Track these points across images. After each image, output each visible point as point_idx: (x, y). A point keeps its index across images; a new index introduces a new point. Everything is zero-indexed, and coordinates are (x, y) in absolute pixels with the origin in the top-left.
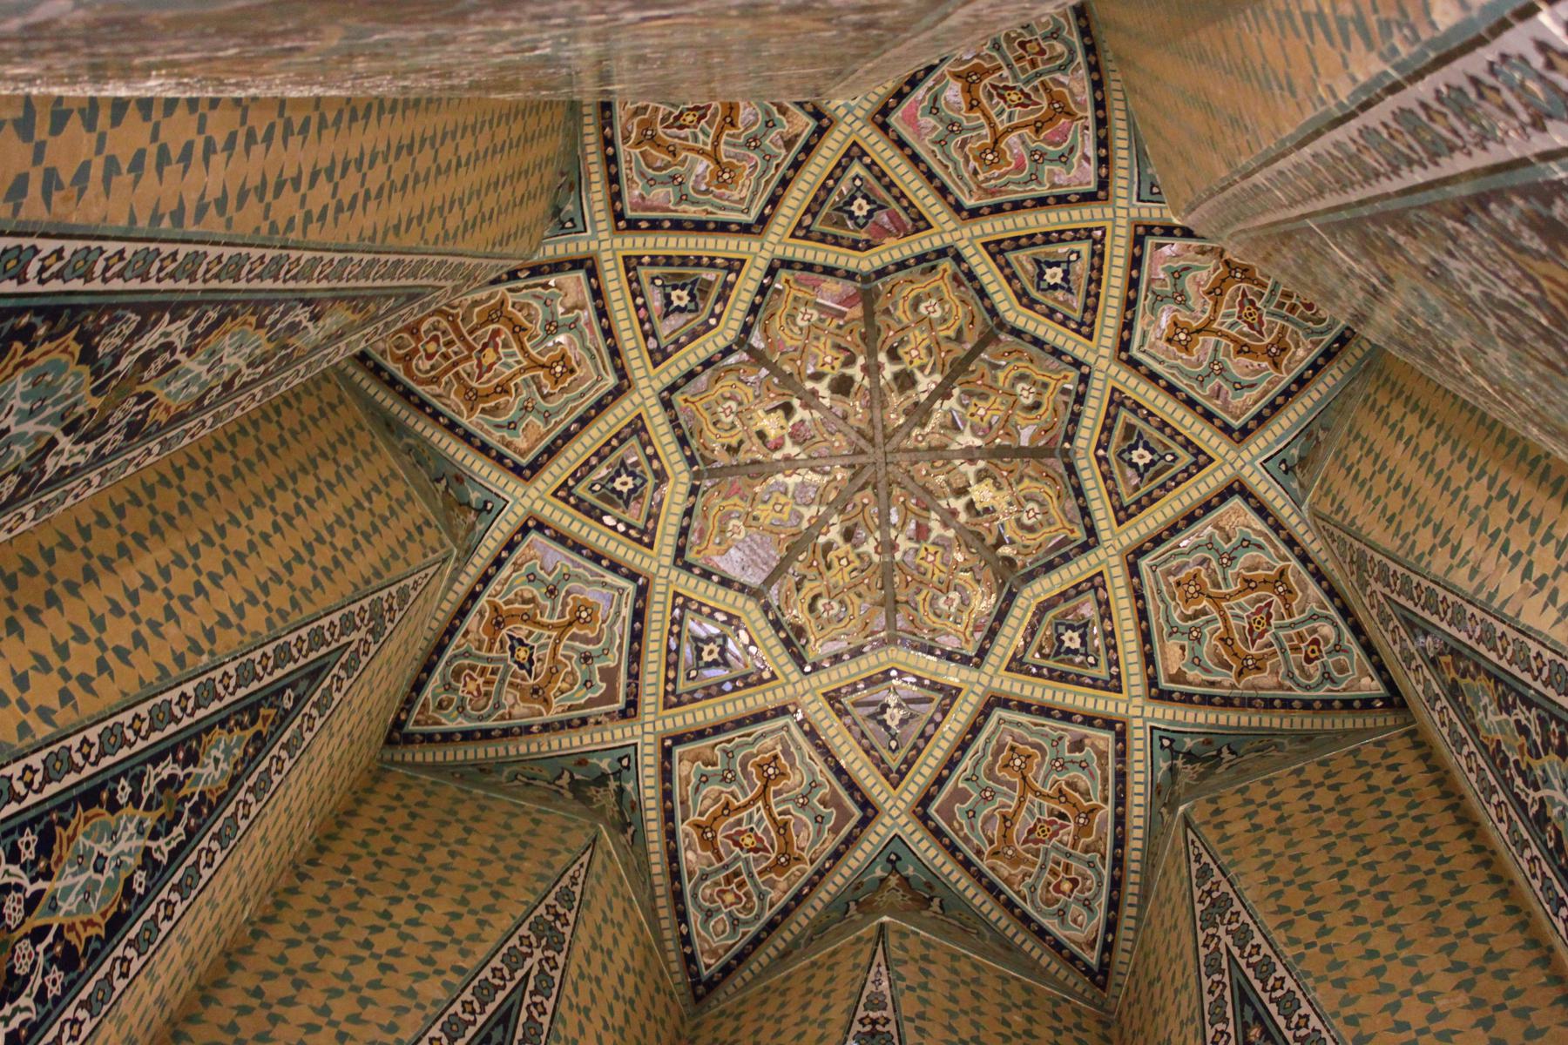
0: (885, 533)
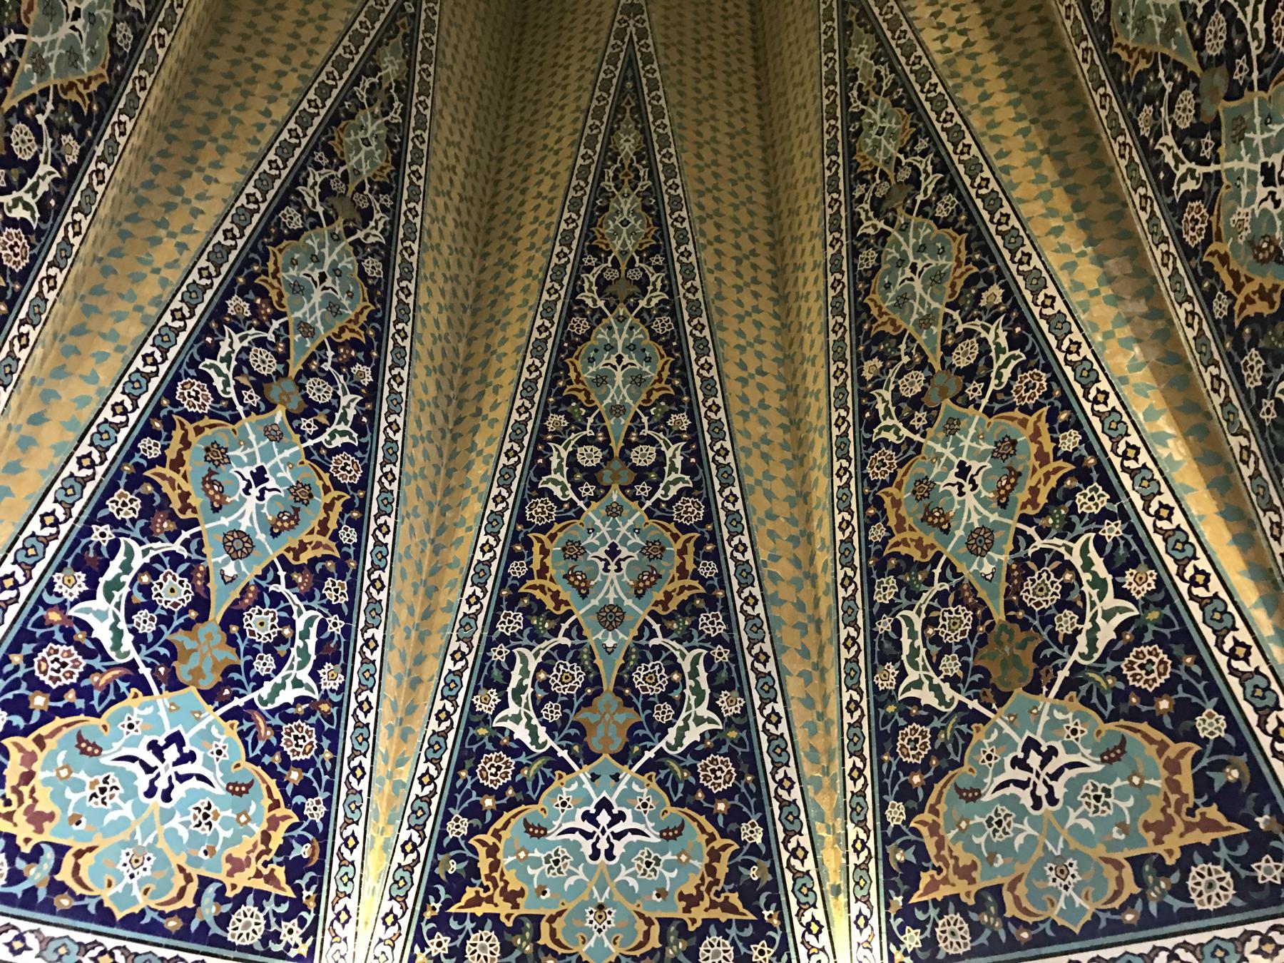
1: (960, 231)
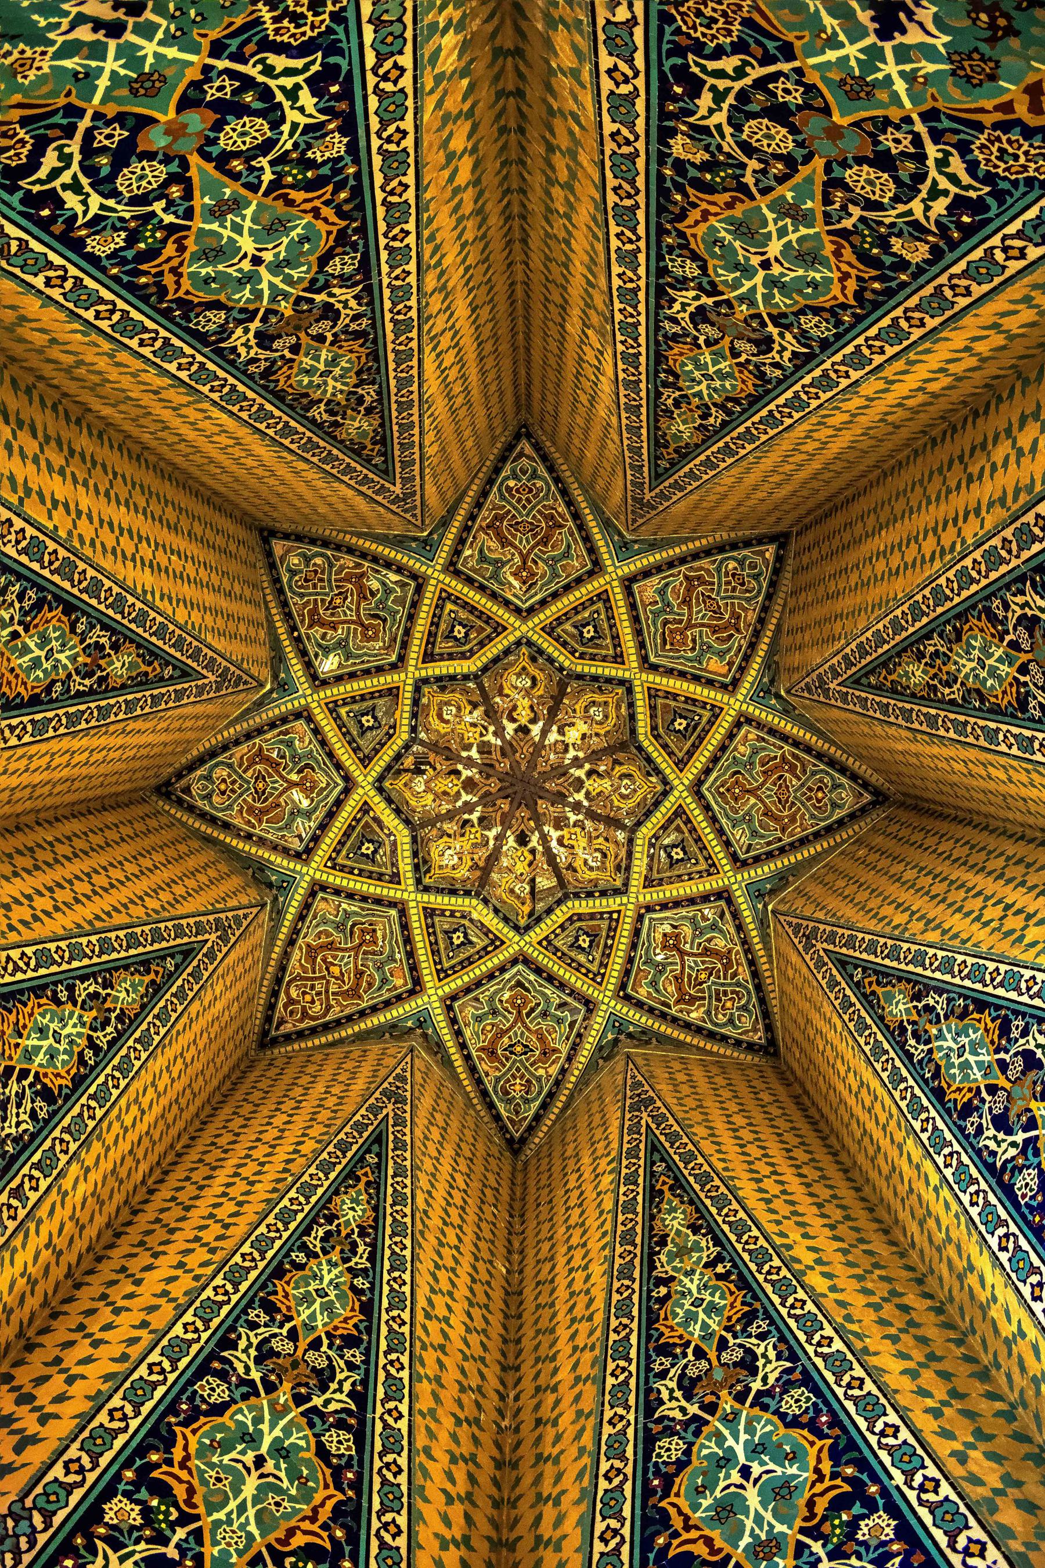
0: (569, 804)
1: (681, 235)
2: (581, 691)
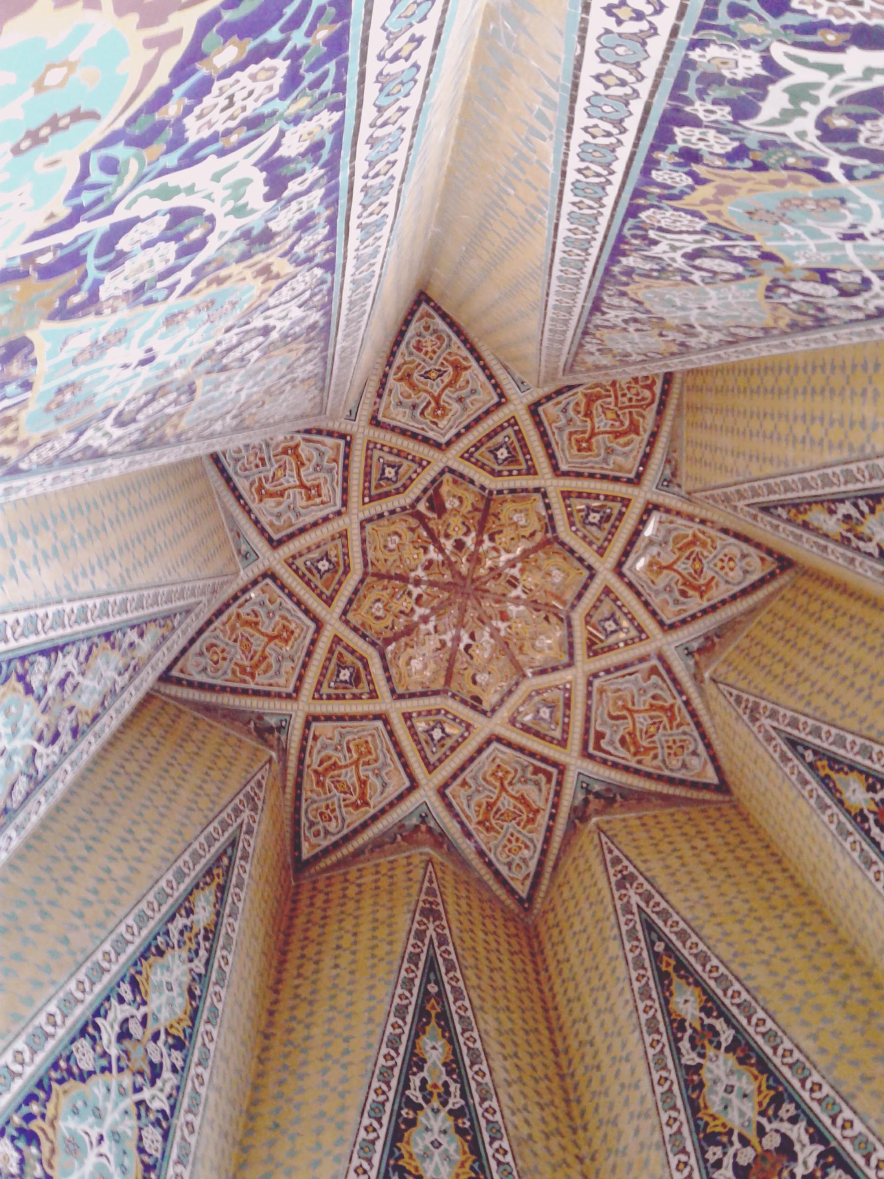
0: (425, 583)
2: (433, 681)
